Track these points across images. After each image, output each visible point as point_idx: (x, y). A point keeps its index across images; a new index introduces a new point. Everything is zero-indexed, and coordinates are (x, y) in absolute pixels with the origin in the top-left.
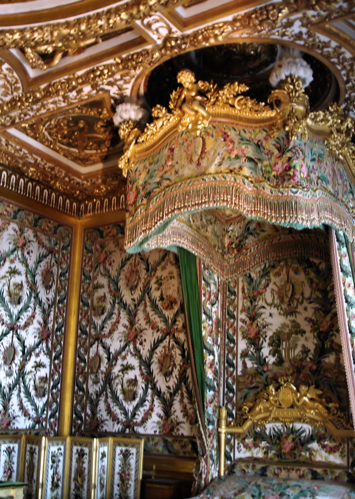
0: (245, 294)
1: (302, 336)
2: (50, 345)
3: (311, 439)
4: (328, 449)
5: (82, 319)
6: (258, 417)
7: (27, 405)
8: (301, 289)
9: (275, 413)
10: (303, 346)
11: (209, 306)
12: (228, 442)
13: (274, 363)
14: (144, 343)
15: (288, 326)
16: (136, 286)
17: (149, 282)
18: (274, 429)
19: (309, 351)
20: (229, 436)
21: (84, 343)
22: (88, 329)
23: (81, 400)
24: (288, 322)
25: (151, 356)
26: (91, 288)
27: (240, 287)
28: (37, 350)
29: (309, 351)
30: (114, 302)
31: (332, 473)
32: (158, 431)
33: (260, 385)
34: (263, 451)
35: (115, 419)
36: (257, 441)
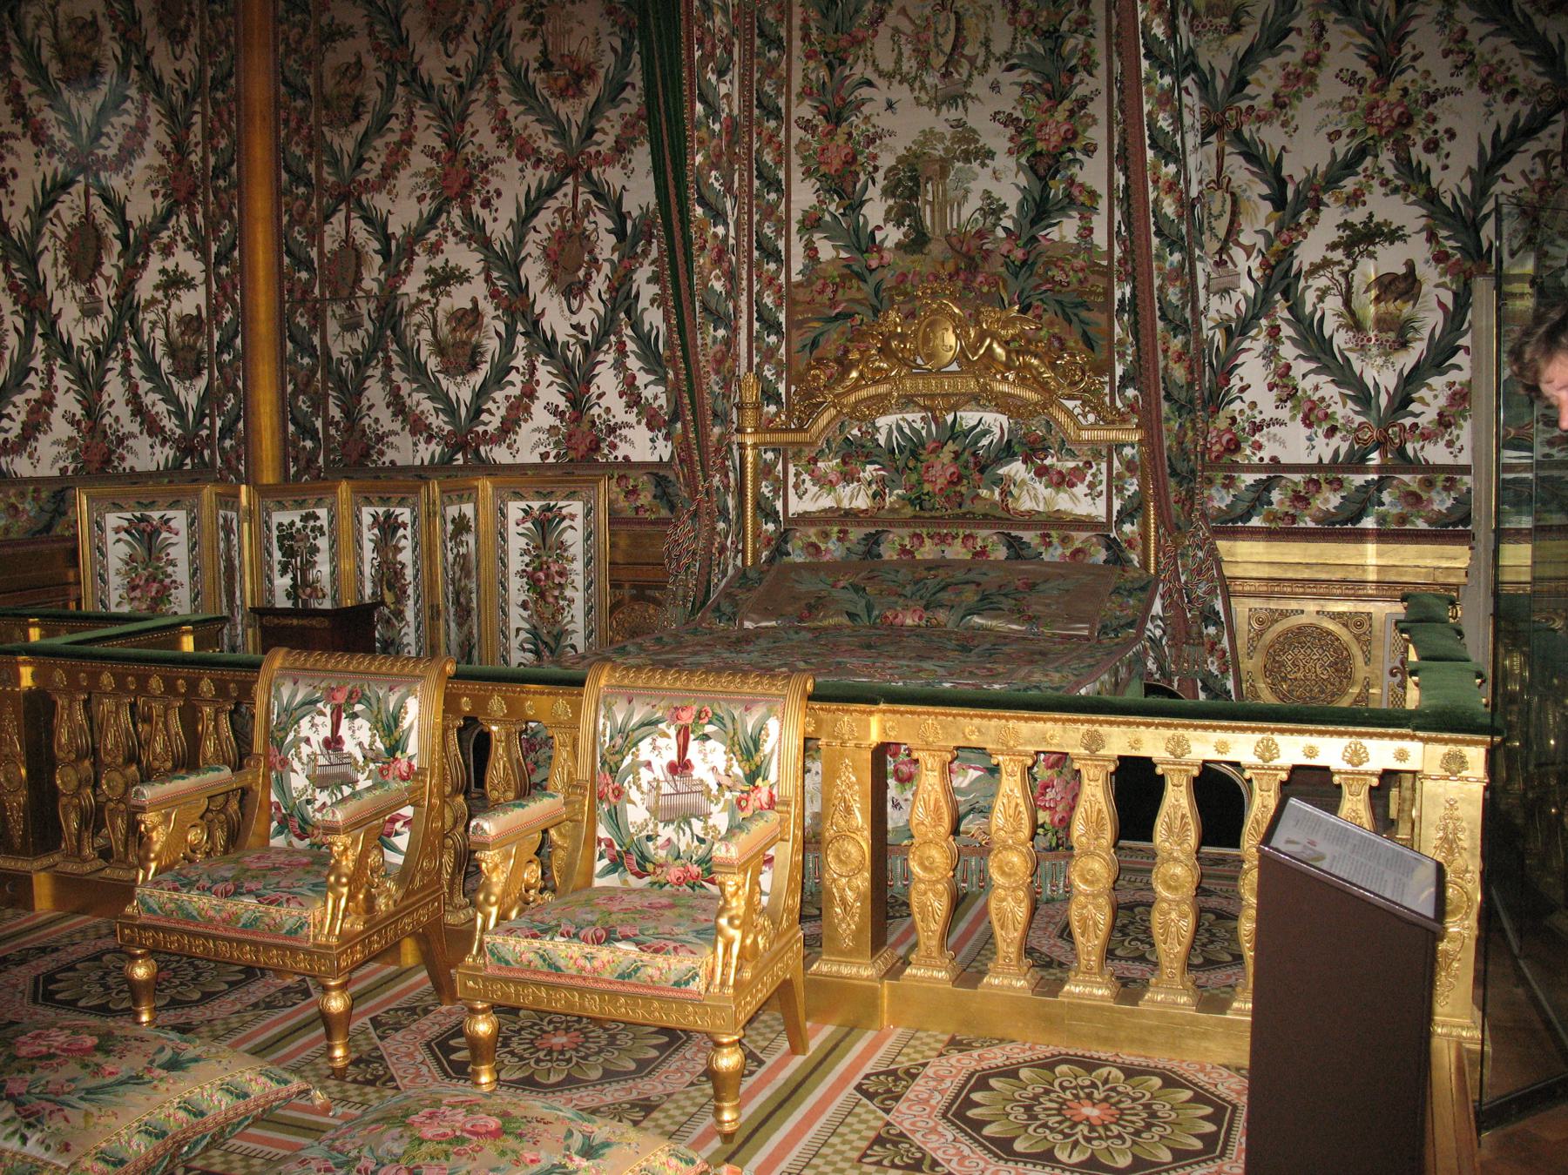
0: (811, 44)
1: (983, 165)
2: (199, 218)
3: (1007, 451)
4: (1055, 478)
5: (289, 138)
6: (852, 399)
7: (154, 402)
8: (982, 27)
10: (987, 195)
11: (713, 78)
12: (765, 471)
13: (899, 246)
14: (495, 202)
15: (942, 138)
16: (460, 30)
17: (502, 15)
18: (900, 429)
19: (1004, 207)
20: (770, 456)
21: (303, 214)
22: (311, 168)
23: (308, 383)
24: (942, 127)
25: (520, 240)
26: (310, 42)
27: (797, 21)
28: (165, 236)
29: (1004, 207)
30: (392, 81)
31: (1065, 540)
32: (553, 454)
33: (858, 308)
34: (870, 492)
35: (418, 426)
36: (854, 464)
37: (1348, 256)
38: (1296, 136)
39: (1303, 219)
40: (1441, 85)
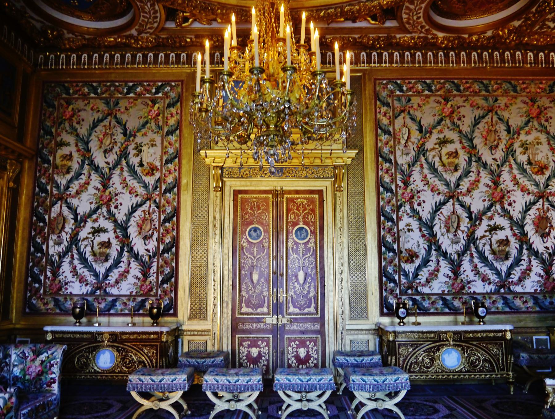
37: (93, 236)
38: (82, 202)
39: (82, 225)
40: (119, 192)
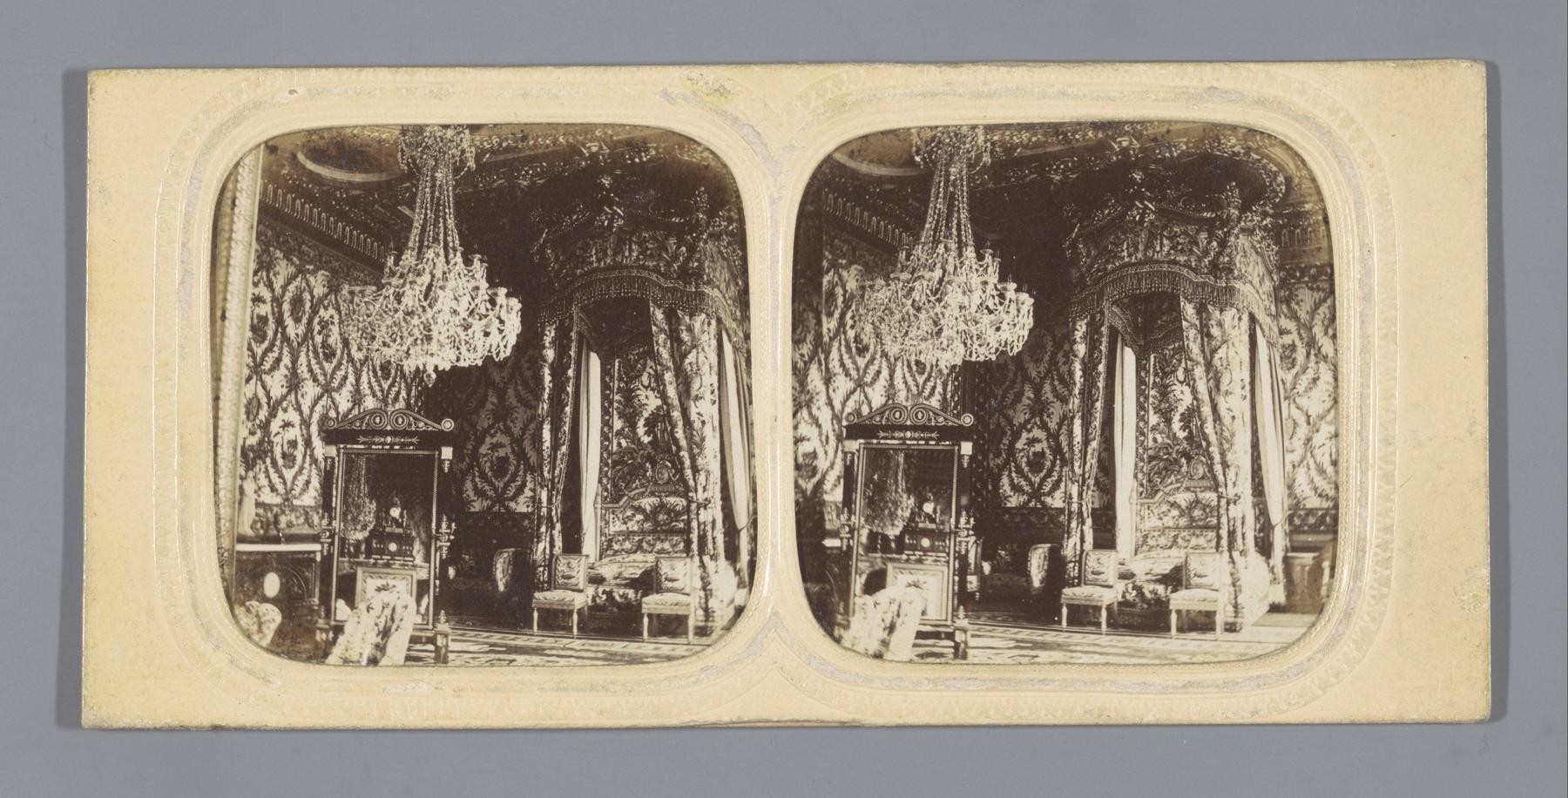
9: (1186, 483)
